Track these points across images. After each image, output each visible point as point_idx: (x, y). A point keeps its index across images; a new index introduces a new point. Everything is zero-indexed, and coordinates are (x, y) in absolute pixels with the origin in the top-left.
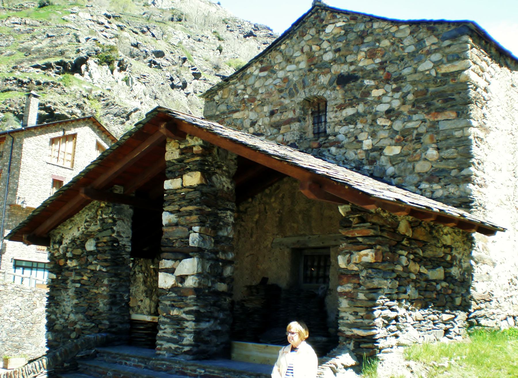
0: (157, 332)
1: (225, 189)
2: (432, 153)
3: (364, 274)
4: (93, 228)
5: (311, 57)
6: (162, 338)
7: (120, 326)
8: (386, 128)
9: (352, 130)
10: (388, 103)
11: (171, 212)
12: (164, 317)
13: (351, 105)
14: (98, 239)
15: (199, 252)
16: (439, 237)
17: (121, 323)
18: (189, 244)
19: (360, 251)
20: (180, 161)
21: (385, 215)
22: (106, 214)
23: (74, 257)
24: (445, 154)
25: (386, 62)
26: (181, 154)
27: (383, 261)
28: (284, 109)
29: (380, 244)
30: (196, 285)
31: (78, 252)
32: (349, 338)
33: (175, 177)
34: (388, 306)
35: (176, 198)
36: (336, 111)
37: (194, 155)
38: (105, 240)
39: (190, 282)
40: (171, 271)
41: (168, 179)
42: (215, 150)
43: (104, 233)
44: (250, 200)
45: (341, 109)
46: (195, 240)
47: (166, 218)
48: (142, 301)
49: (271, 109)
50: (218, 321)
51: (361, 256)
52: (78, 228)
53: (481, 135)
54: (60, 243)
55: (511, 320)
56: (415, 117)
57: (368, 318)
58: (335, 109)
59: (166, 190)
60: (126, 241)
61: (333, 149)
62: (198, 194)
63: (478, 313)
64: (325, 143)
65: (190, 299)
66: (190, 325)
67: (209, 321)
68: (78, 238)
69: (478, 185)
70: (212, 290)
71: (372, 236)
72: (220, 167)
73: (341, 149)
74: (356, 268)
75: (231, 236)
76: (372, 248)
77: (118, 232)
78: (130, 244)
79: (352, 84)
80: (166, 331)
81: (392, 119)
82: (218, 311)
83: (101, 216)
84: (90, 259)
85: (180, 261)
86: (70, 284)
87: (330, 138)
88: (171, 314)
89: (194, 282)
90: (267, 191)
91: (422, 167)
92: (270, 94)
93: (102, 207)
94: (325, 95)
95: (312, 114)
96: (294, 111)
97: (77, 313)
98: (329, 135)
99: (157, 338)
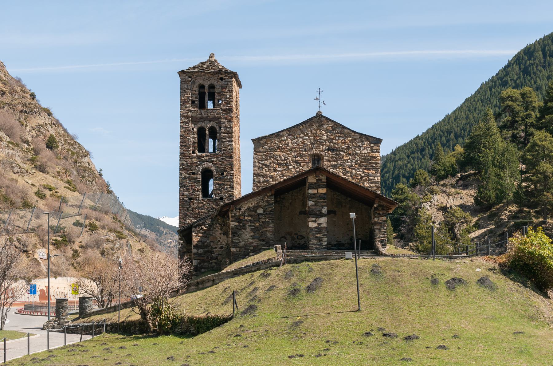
5: (315, 135)
11: (313, 201)
13: (334, 161)
25: (349, 147)
40: (315, 221)
47: (310, 203)
48: (220, 238)
54: (240, 209)
79: (336, 152)
84: (260, 217)
86: (247, 226)
92: (295, 148)
97: (253, 239)
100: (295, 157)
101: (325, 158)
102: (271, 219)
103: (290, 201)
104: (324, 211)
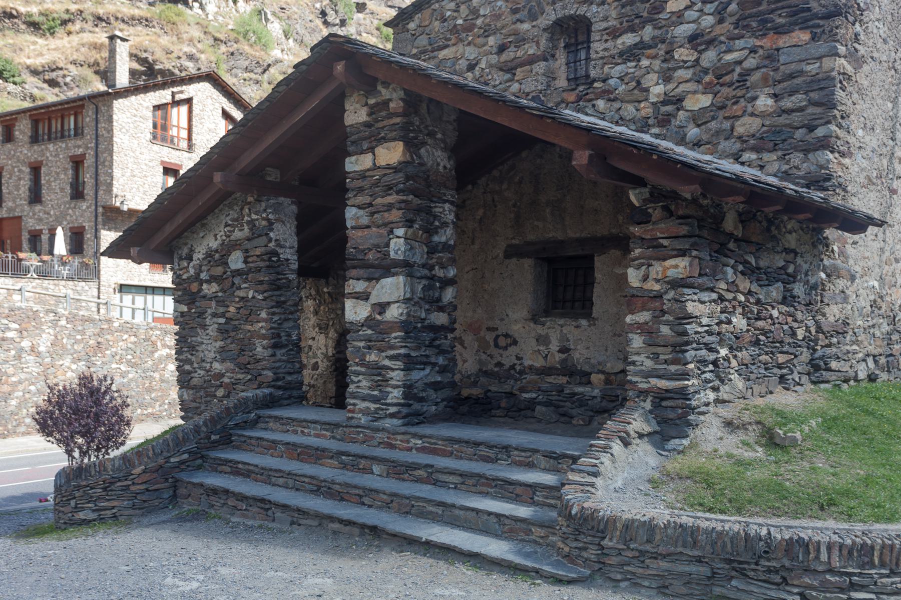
0: (347, 386)
1: (441, 168)
2: (764, 102)
3: (671, 294)
4: (237, 234)
6: (354, 396)
7: (289, 378)
8: (689, 64)
9: (632, 70)
10: (693, 22)
11: (359, 207)
12: (357, 364)
13: (632, 29)
14: (247, 251)
15: (406, 266)
16: (779, 236)
17: (290, 373)
18: (389, 255)
19: (665, 260)
20: (367, 125)
21: (706, 202)
22: (256, 214)
23: (213, 279)
24: (787, 103)
26: (370, 114)
27: (700, 275)
28: (520, 40)
29: (694, 246)
30: (403, 318)
31: (219, 271)
32: (643, 393)
33: (362, 152)
34: (704, 344)
35: (365, 183)
36: (606, 41)
37: (391, 115)
38: (258, 252)
39: (394, 313)
40: (364, 296)
41: (350, 155)
42: (424, 106)
43: (256, 242)
44: (470, 187)
45: (615, 37)
46: (399, 249)
47: (351, 213)
48: (313, 339)
49: (500, 42)
50: (437, 368)
51: (665, 269)
52: (215, 236)
53: (849, 69)
55: (870, 361)
56: (739, 43)
57: (675, 362)
58: (605, 37)
59: (349, 173)
60: (289, 254)
61: (601, 104)
62: (400, 177)
63: (828, 351)
64: (587, 94)
65: (395, 338)
66: (397, 376)
67: (423, 369)
68: (216, 251)
69: (839, 152)
70: (426, 324)
71: (684, 236)
72: (431, 134)
73: (613, 103)
74: (657, 287)
75: (452, 242)
76: (684, 255)
77: (276, 240)
78: (296, 257)
80: (360, 384)
81: (700, 48)
82: (438, 354)
83: (249, 215)
84: (237, 280)
85: (378, 280)
87: (596, 85)
88: (367, 359)
89: (400, 311)
90: (496, 173)
91: (746, 126)
93: (249, 203)
94: (588, 15)
95: (565, 47)
96: (538, 43)
98: (594, 81)
99: (347, 395)
100: (502, 49)
101: (595, 27)
102: (260, 287)
103: (481, 212)
104: (397, 247)
